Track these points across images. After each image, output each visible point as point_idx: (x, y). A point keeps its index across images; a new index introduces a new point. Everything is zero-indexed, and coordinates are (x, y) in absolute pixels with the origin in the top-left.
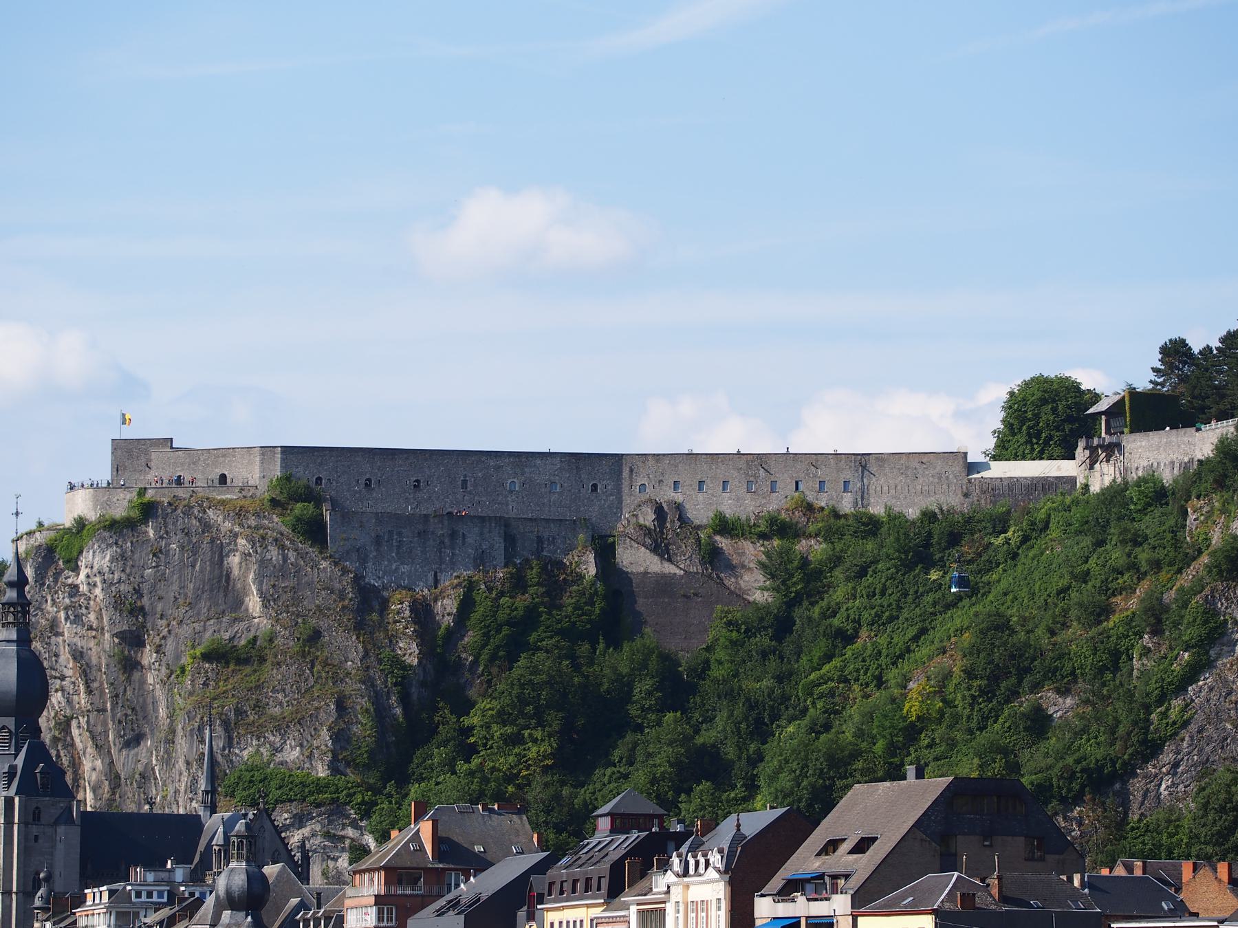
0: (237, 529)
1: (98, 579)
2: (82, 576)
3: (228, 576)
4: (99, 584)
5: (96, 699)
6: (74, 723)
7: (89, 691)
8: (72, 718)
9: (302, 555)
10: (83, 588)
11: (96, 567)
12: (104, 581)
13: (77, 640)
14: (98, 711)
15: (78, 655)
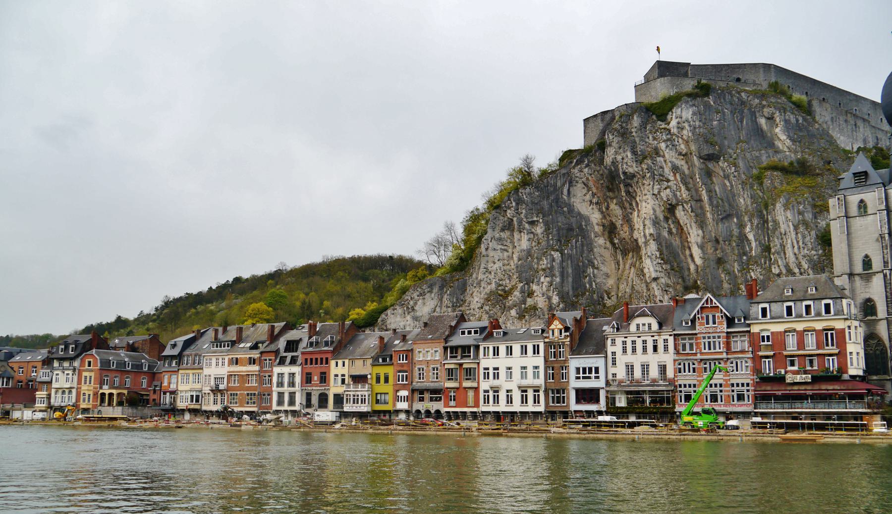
0: (764, 103)
1: (686, 125)
2: (673, 123)
3: (762, 130)
4: (687, 127)
5: (694, 193)
6: (680, 207)
7: (688, 189)
8: (678, 205)
9: (805, 119)
10: (674, 131)
11: (684, 118)
12: (690, 126)
13: (674, 160)
14: (696, 201)
15: (675, 169)
